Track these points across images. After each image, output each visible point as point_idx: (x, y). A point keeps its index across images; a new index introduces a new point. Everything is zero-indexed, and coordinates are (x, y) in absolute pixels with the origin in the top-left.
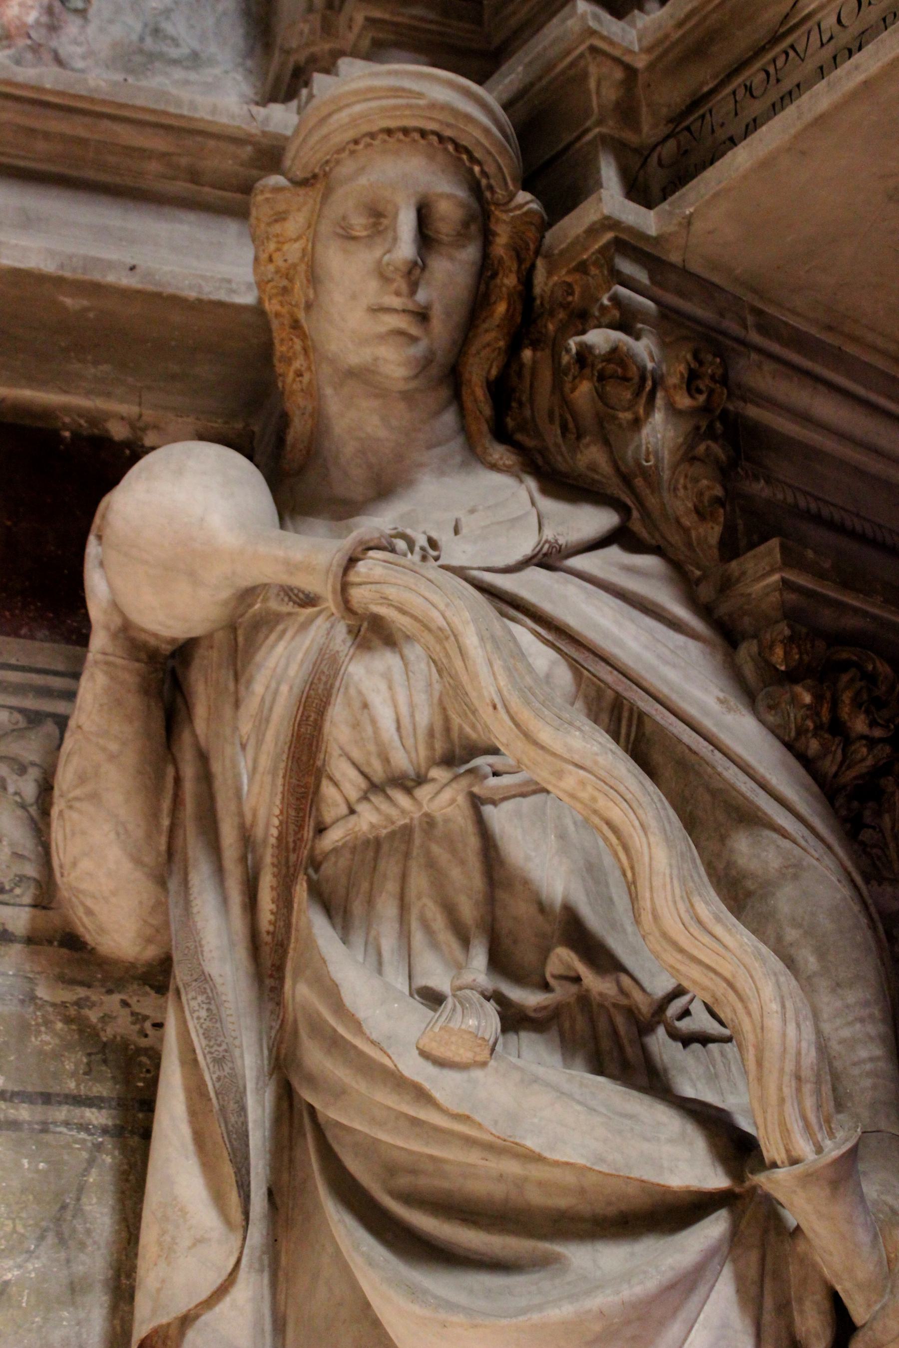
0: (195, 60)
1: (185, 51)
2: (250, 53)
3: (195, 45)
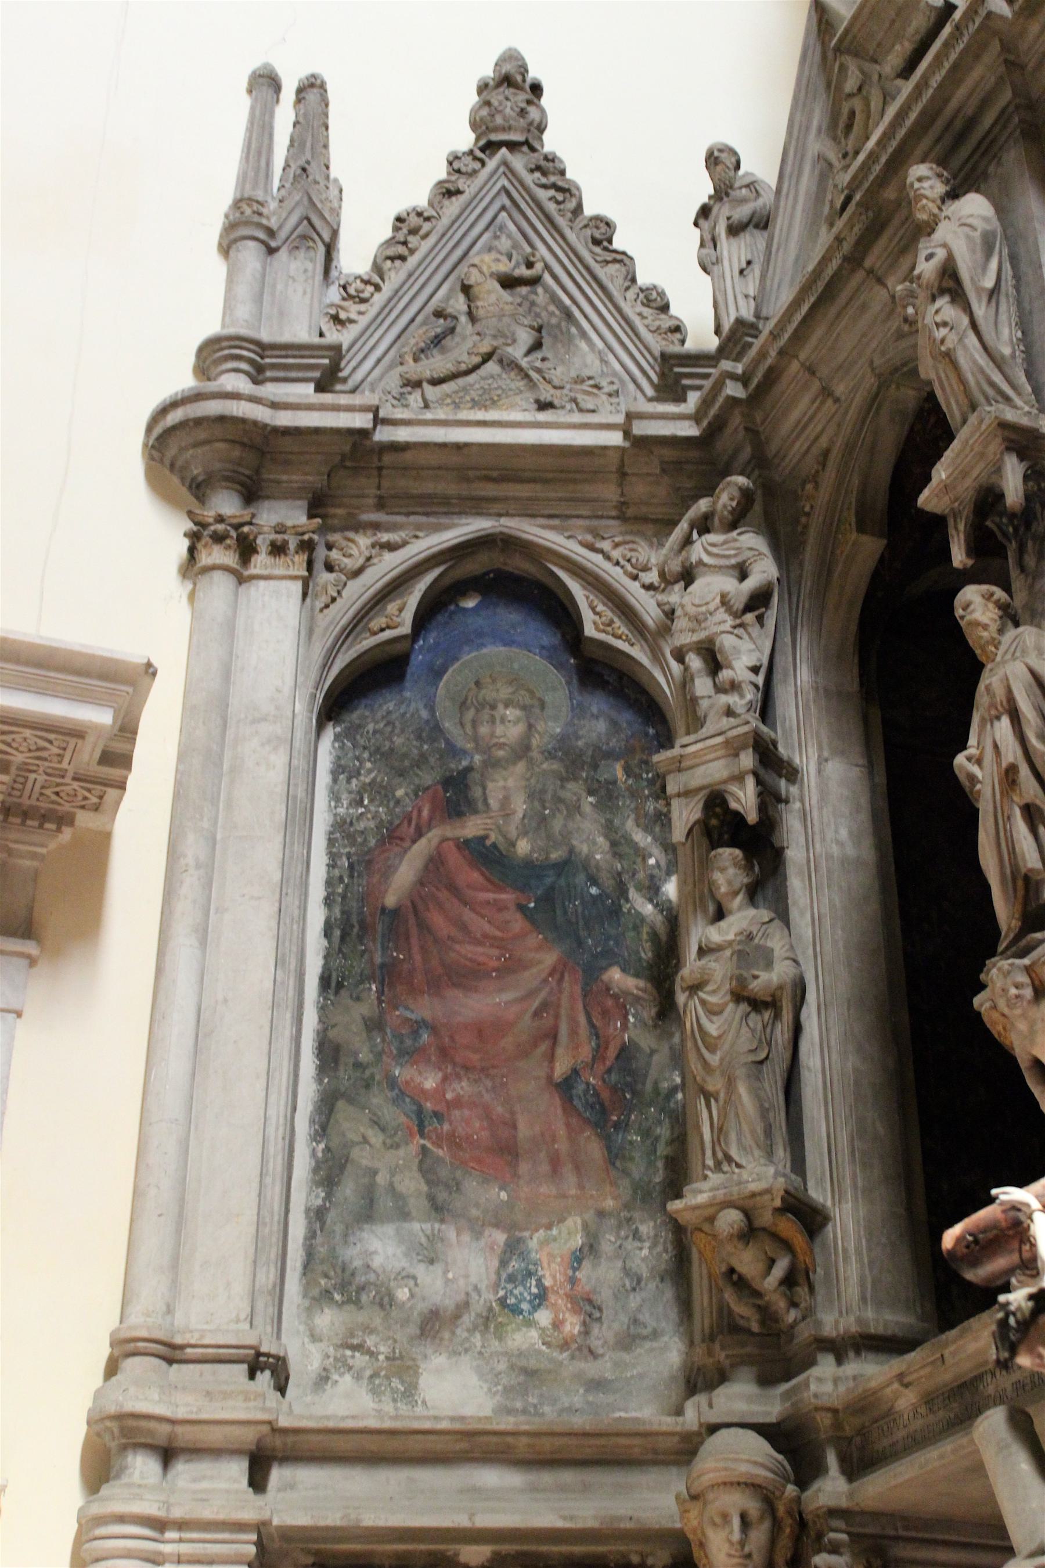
0: (655, 1335)
1: (649, 1330)
2: (681, 1323)
3: (654, 1324)
